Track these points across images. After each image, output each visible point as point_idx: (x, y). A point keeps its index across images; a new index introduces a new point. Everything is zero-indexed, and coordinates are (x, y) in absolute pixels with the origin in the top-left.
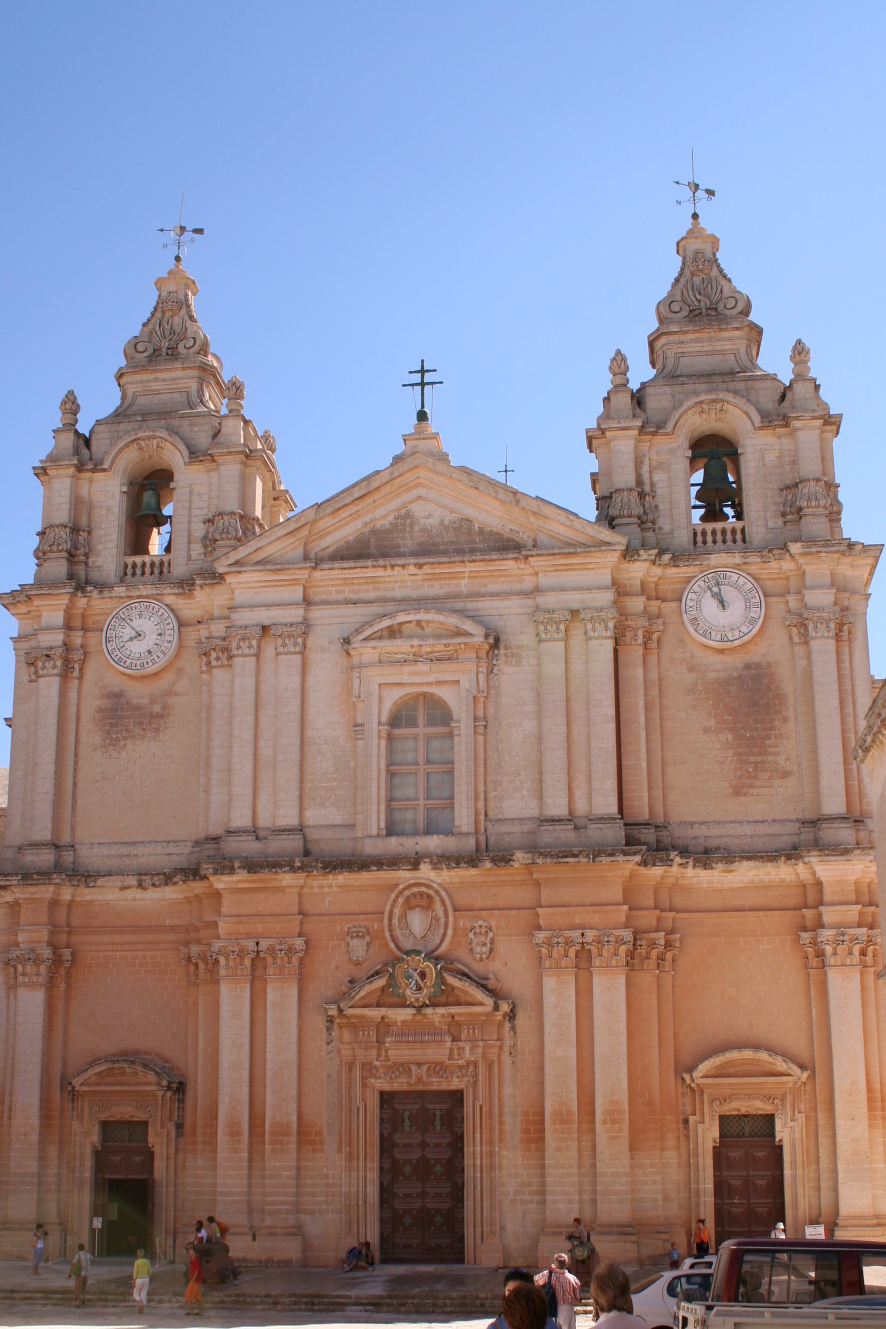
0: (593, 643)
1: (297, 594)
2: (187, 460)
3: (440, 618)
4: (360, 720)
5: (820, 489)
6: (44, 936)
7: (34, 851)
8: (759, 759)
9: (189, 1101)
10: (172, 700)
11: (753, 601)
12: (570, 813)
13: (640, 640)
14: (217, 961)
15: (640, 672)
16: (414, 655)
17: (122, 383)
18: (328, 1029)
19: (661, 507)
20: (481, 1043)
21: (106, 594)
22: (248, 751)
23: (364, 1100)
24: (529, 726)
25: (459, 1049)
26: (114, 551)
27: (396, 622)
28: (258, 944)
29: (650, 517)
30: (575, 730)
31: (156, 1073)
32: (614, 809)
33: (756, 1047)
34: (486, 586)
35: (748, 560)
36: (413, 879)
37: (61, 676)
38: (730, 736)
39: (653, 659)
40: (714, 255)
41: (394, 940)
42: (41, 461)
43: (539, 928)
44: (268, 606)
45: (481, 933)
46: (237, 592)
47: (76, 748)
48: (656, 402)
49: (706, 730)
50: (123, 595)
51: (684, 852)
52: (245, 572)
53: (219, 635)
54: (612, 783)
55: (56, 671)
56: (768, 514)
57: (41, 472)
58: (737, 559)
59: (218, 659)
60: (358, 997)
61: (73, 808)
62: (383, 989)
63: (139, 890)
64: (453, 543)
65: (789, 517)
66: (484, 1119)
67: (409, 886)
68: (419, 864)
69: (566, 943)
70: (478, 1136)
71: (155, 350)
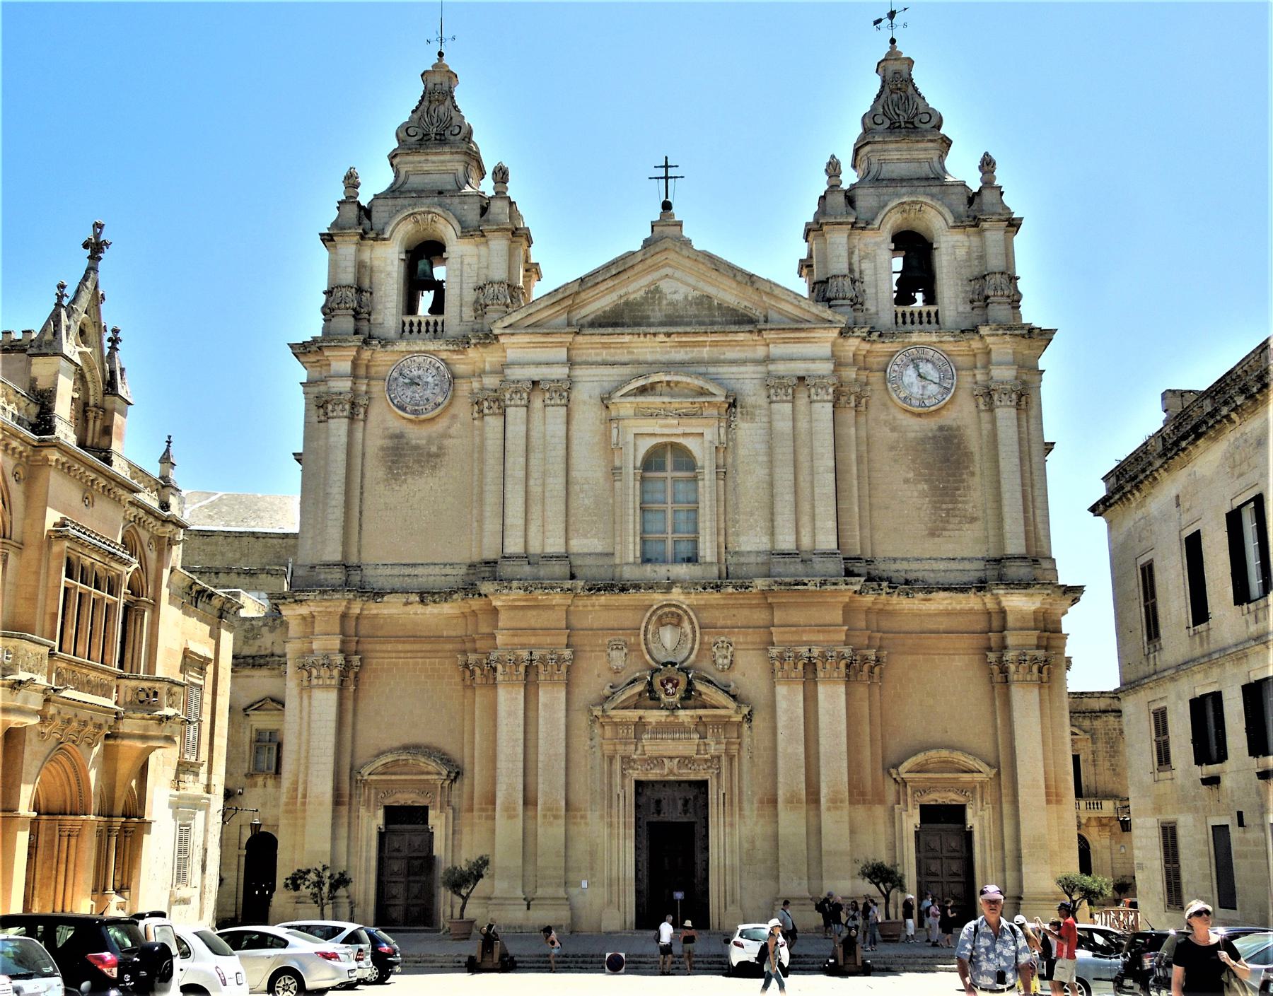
0: (816, 405)
1: (562, 354)
2: (459, 234)
3: (689, 380)
4: (617, 463)
5: (1004, 280)
6: (336, 643)
8: (950, 506)
10: (446, 442)
13: (853, 404)
14: (495, 670)
15: (853, 430)
17: (394, 163)
18: (591, 727)
19: (867, 291)
21: (389, 348)
23: (623, 787)
24: (761, 472)
26: (394, 311)
28: (531, 653)
29: (860, 300)
30: (801, 478)
32: (834, 546)
33: (952, 748)
35: (943, 339)
38: (926, 487)
39: (862, 419)
40: (910, 75)
41: (649, 653)
43: (773, 644)
44: (538, 364)
47: (362, 481)
48: (866, 200)
49: (906, 481)
53: (491, 387)
54: (831, 524)
55: (345, 414)
56: (959, 301)
57: (327, 238)
58: (934, 338)
59: (489, 408)
60: (619, 701)
61: (360, 533)
62: (640, 694)
64: (696, 316)
67: (661, 607)
69: (796, 657)
71: (424, 135)
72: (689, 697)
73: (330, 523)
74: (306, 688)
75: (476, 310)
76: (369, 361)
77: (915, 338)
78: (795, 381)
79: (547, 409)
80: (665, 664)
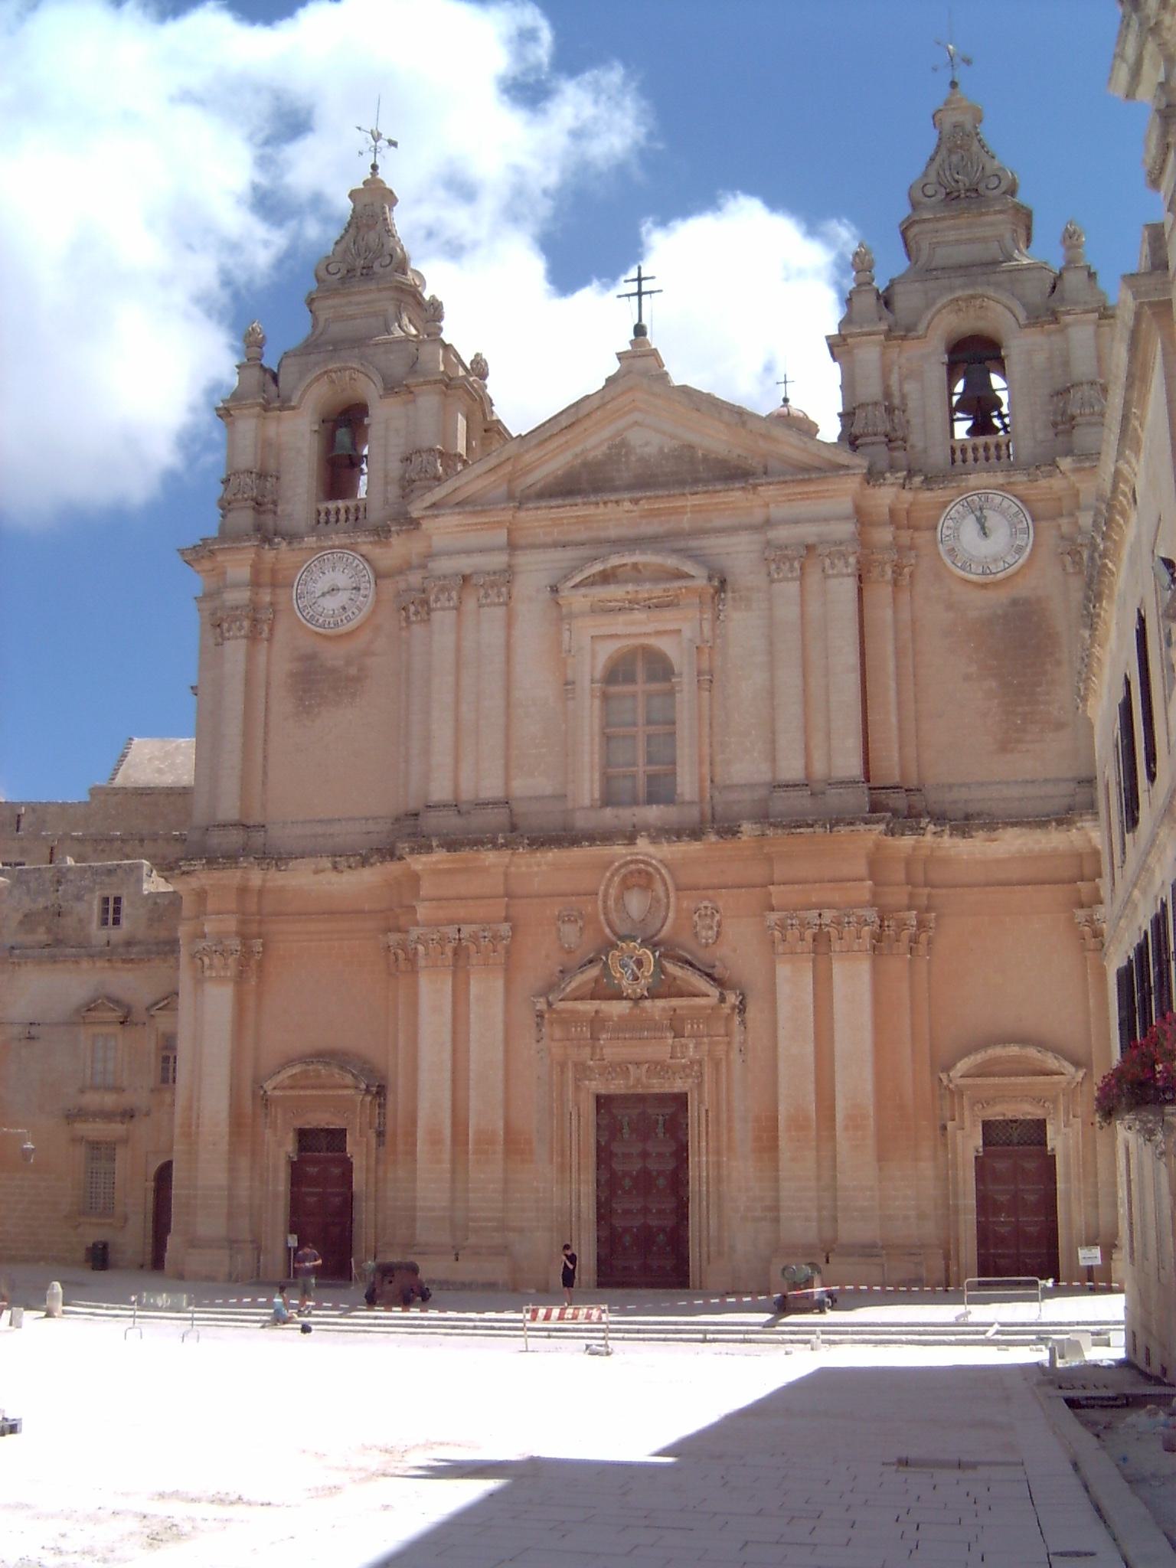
0: (833, 583)
1: (501, 537)
4: (570, 676)
6: (231, 924)
8: (1027, 709)
9: (390, 1106)
11: (1020, 526)
15: (888, 614)
16: (630, 602)
17: (313, 309)
18: (538, 1025)
20: (705, 1040)
21: (296, 545)
23: (577, 1104)
25: (682, 1046)
27: (609, 565)
28: (459, 930)
29: (900, 434)
31: (353, 1075)
33: (1023, 1041)
35: (1012, 480)
36: (631, 854)
37: (246, 637)
39: (905, 597)
45: (706, 915)
46: (434, 537)
47: (266, 716)
49: (967, 678)
50: (315, 546)
51: (940, 818)
52: (443, 515)
55: (243, 633)
58: (1000, 479)
60: (568, 989)
61: (264, 784)
62: (597, 981)
63: (335, 873)
65: (1060, 427)
68: (636, 839)
70: (704, 1144)
74: (199, 982)
75: (403, 488)
76: (274, 564)
77: (973, 480)
78: (804, 552)
79: (482, 610)
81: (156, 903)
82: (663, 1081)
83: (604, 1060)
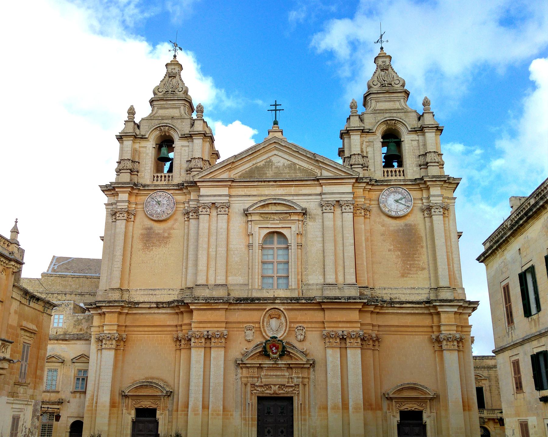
7: (112, 292)
8: (411, 262)
10: (172, 231)
12: (336, 281)
13: (363, 214)
14: (190, 340)
22: (205, 253)
23: (251, 399)
28: (208, 332)
29: (366, 165)
32: (354, 281)
34: (301, 190)
42: (120, 133)
49: (390, 250)
54: (353, 270)
57: (120, 138)
62: (260, 352)
64: (288, 173)
65: (422, 167)
66: (302, 410)
72: (284, 353)
73: (115, 269)
78: (335, 202)
80: (272, 338)
81: (78, 318)
82: (284, 392)
83: (262, 383)
